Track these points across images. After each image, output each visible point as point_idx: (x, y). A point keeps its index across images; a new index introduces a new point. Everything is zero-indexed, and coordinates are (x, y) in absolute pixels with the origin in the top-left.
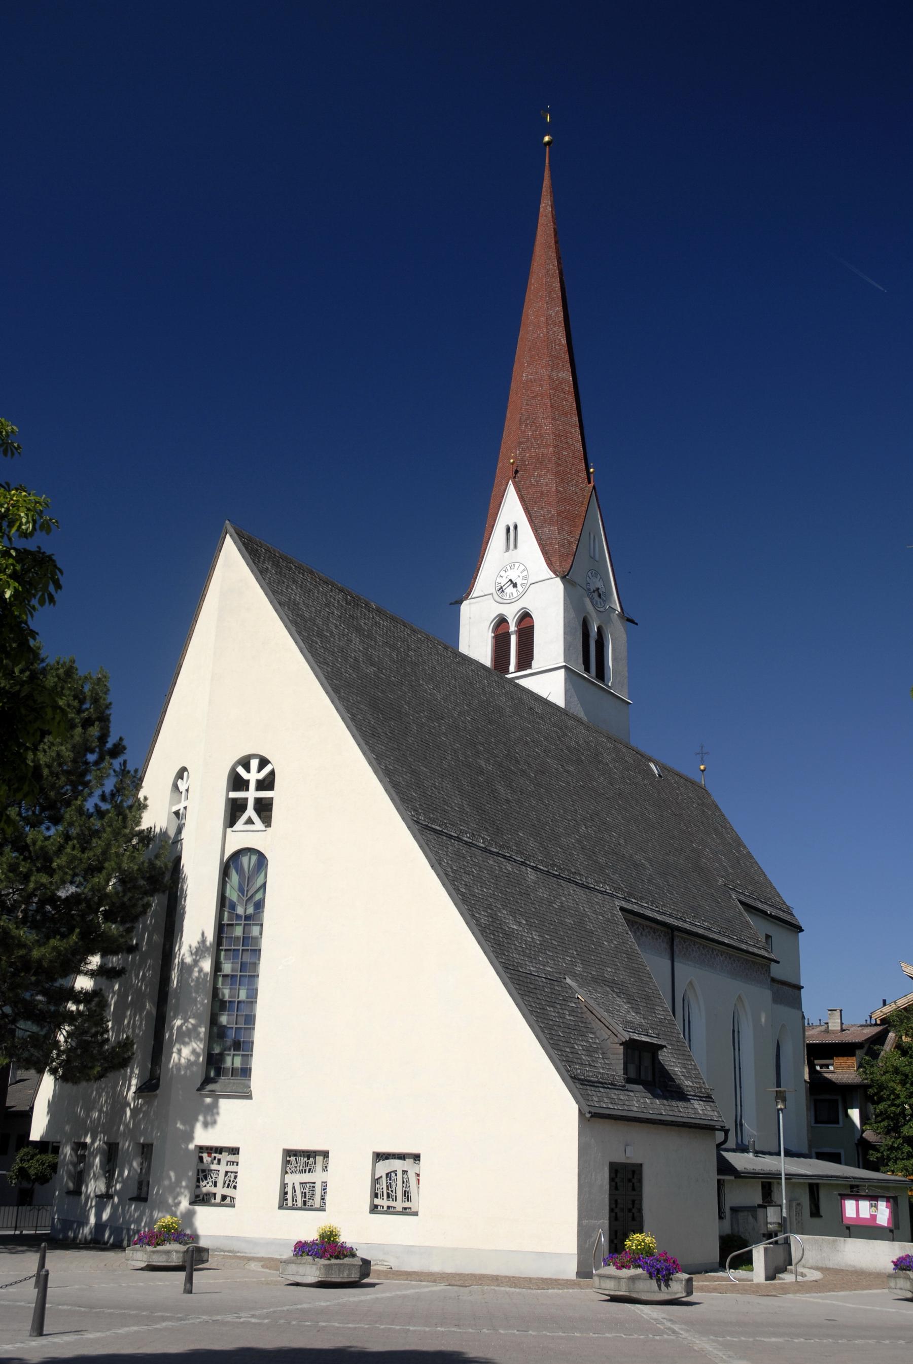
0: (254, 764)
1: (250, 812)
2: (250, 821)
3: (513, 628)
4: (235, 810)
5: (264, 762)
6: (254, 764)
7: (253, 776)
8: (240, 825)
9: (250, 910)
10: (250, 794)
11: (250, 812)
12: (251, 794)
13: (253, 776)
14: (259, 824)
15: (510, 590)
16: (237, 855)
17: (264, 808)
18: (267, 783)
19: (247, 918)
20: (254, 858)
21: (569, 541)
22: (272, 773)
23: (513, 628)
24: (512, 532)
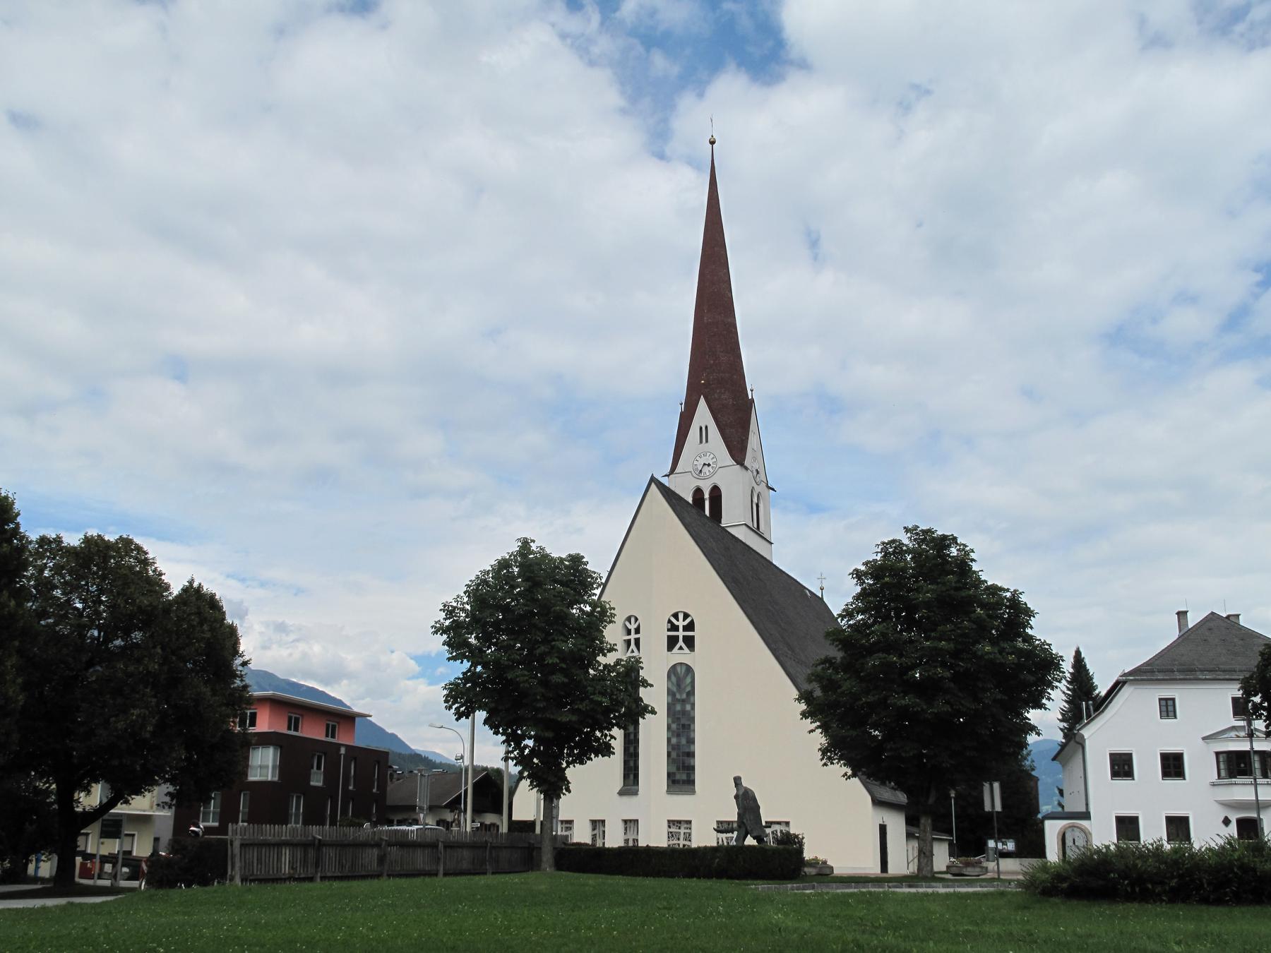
0: (681, 616)
1: (681, 643)
2: (681, 648)
3: (707, 496)
4: (672, 642)
5: (686, 616)
6: (681, 616)
7: (681, 623)
8: (676, 650)
9: (684, 696)
10: (682, 634)
11: (681, 643)
12: (681, 633)
13: (681, 623)
14: (686, 650)
15: (706, 469)
16: (674, 667)
17: (690, 642)
18: (690, 627)
19: (683, 701)
20: (684, 668)
21: (1202, 884)
22: (692, 622)
23: (707, 496)
24: (704, 432)
